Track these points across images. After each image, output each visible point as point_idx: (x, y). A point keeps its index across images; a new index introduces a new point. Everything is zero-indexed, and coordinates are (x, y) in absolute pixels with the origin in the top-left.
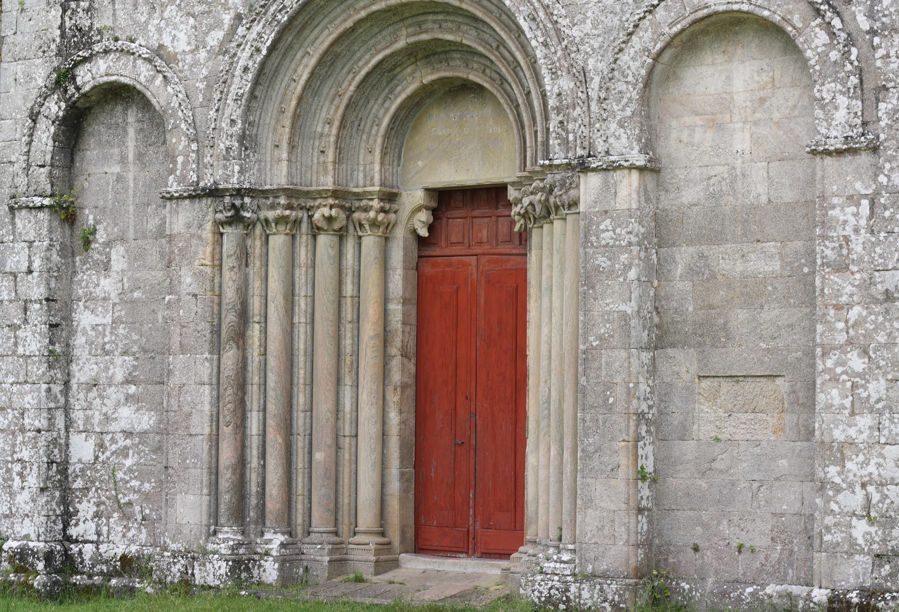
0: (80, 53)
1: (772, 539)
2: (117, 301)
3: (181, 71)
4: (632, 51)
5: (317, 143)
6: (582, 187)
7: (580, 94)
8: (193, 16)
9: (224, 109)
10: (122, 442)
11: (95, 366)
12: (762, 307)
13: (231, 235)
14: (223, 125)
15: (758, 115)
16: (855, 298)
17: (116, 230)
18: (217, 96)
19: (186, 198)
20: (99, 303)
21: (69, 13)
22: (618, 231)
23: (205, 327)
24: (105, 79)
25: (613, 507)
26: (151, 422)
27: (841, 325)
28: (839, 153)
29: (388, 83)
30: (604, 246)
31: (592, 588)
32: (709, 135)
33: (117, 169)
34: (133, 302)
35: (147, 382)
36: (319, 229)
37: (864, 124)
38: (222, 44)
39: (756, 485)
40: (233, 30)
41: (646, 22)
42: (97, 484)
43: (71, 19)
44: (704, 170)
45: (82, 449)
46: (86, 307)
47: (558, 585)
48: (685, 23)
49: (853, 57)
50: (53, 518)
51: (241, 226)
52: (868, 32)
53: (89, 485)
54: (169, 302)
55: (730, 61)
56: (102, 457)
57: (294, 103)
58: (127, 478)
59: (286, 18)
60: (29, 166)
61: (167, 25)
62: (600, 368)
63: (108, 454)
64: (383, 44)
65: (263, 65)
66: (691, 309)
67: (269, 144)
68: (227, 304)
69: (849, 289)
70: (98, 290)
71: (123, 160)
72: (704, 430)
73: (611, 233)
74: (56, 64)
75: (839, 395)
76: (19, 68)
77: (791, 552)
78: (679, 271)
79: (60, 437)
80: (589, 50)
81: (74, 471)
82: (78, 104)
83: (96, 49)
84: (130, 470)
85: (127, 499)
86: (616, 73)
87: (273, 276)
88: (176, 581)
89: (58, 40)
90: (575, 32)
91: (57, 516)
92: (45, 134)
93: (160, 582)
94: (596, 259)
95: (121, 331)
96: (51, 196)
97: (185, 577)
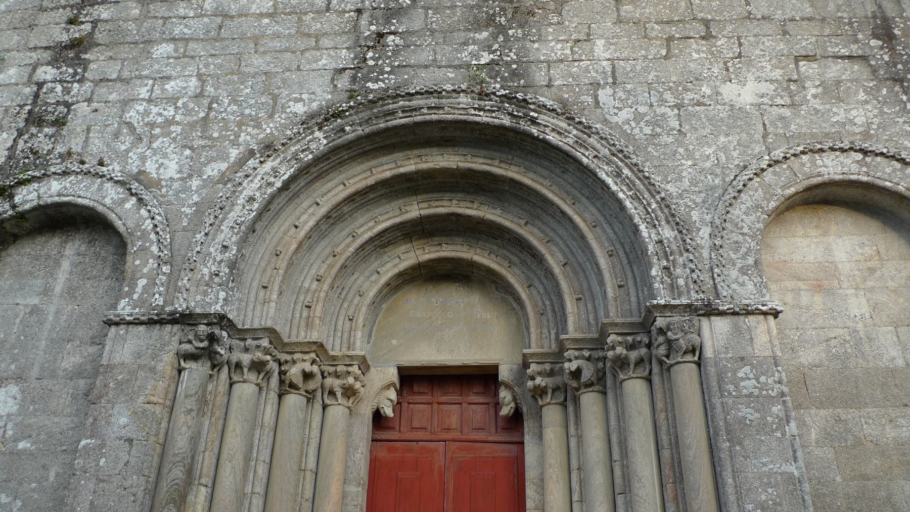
0: (30, 173)
3: (162, 196)
4: (743, 207)
5: (302, 298)
6: (706, 332)
9: (215, 234)
13: (196, 371)
14: (212, 250)
15: (870, 284)
17: (13, 367)
19: (142, 323)
21: (26, 137)
22: (763, 379)
24: (56, 199)
32: (818, 299)
33: (35, 301)
36: (292, 386)
40: (241, 162)
43: (26, 142)
44: (821, 332)
48: (800, 187)
51: (209, 364)
55: (825, 234)
57: (294, 246)
59: (310, 157)
61: (154, 154)
64: (391, 214)
65: (273, 197)
67: (255, 284)
68: (174, 455)
71: (46, 292)
73: (754, 381)
78: (813, 436)
80: (690, 204)
83: (53, 169)
86: (728, 225)
87: (234, 430)
90: (671, 188)
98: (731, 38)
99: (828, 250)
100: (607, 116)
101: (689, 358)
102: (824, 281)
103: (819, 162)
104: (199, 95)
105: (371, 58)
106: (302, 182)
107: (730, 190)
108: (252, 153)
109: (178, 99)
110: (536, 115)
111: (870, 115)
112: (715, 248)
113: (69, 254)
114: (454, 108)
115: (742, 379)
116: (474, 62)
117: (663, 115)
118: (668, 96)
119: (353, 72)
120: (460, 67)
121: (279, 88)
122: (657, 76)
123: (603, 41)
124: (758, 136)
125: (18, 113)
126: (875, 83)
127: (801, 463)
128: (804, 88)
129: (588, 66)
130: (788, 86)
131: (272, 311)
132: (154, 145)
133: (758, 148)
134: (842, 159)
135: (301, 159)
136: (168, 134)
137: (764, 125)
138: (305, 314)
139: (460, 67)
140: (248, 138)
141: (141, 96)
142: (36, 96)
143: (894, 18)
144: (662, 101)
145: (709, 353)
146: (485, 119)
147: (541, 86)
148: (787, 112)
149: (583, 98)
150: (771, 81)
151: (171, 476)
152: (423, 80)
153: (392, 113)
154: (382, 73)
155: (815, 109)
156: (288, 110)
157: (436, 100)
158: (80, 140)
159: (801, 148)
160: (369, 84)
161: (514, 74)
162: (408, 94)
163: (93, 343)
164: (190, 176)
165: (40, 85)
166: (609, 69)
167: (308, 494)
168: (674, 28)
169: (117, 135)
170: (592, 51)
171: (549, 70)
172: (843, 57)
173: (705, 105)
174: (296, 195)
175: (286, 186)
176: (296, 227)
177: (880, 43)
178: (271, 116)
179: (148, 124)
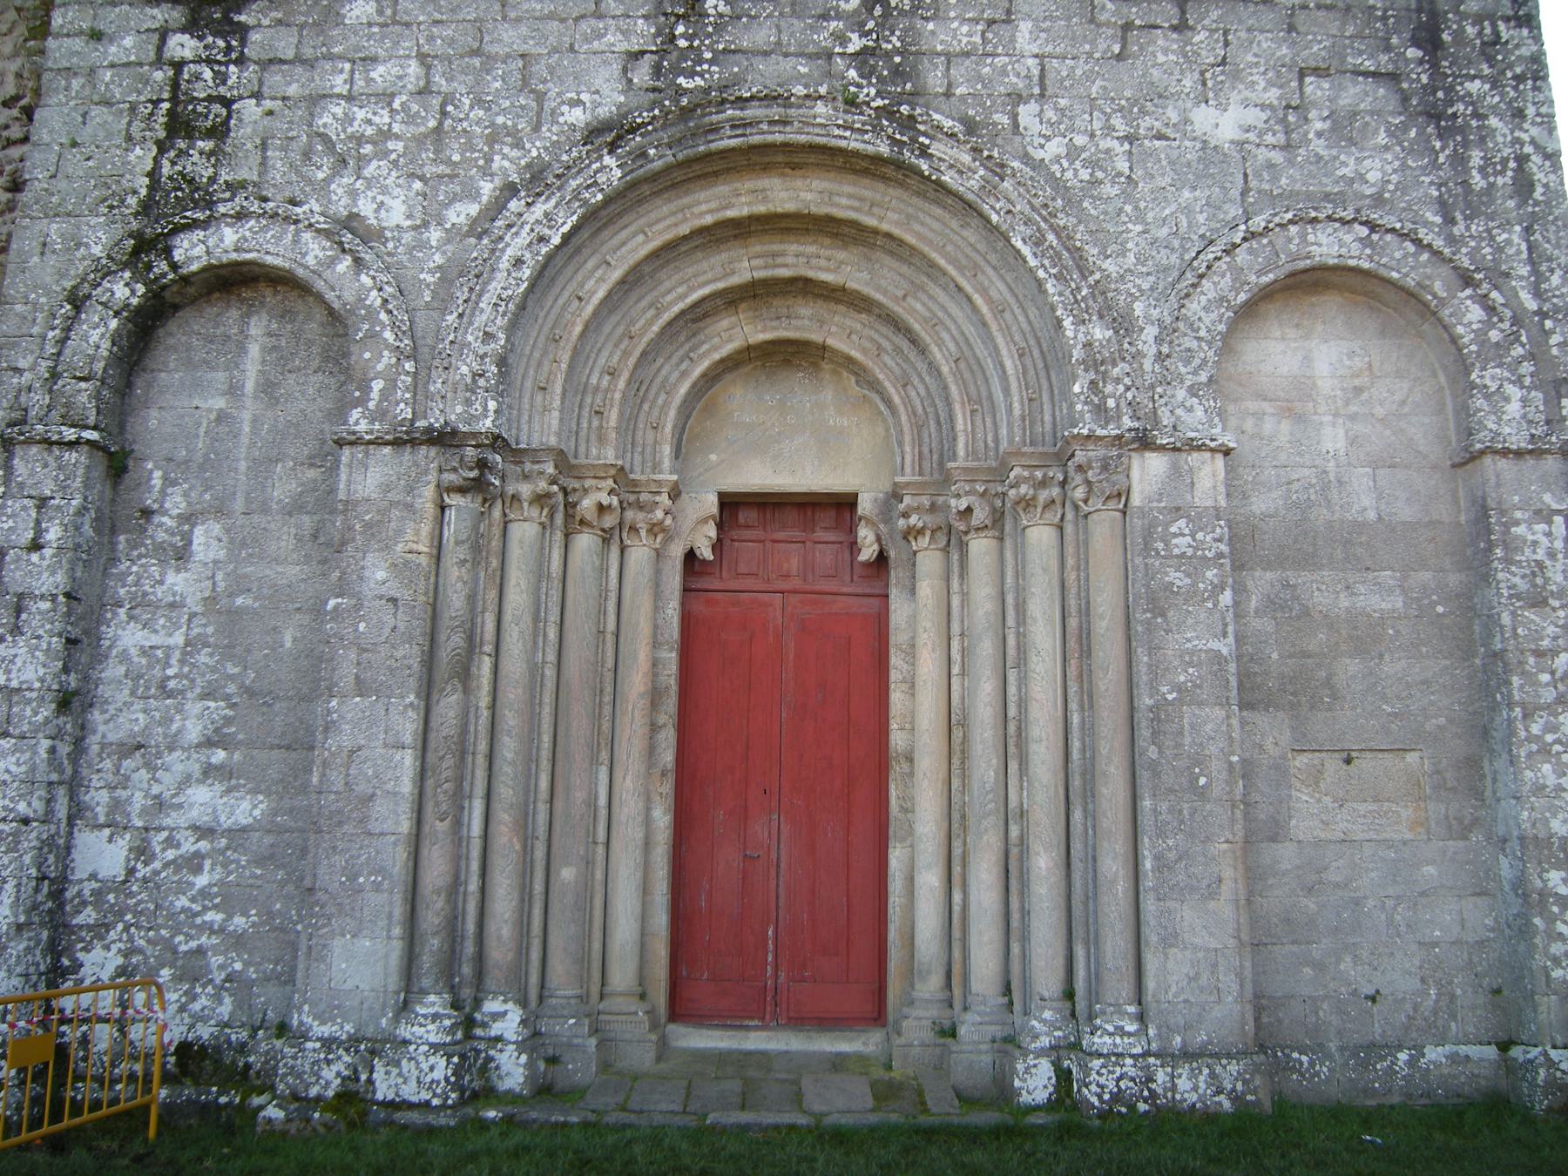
0: (188, 214)
1: (1423, 980)
2: (199, 609)
3: (389, 254)
4: (1203, 299)
5: (589, 400)
6: (1135, 474)
7: (1126, 346)
8: (422, 178)
9: (473, 314)
10: (189, 846)
11: (141, 716)
12: (1381, 656)
14: (470, 338)
15: (1353, 408)
16: (1561, 641)
17: (207, 497)
18: (462, 295)
19: (387, 443)
20: (160, 612)
21: (172, 154)
22: (1200, 536)
23: (410, 654)
24: (234, 256)
25: (1213, 944)
26: (257, 812)
27: (1545, 678)
28: (1519, 454)
29: (688, 339)
30: (1177, 556)
31: (1193, 1075)
32: (1285, 426)
33: (220, 403)
34: (235, 614)
35: (250, 744)
37: (1548, 422)
38: (474, 222)
39: (1390, 903)
40: (496, 207)
41: (1222, 265)
42: (128, 917)
43: (173, 163)
44: (1282, 472)
45: (101, 855)
46: (131, 618)
47: (1132, 1072)
48: (1281, 273)
49: (1524, 339)
50: (35, 978)
51: (480, 499)
52: (1535, 313)
53: (110, 918)
54: (336, 608)
55: (1307, 337)
56: (143, 870)
57: (578, 329)
58: (197, 907)
59: (600, 197)
60: (54, 375)
61: (369, 188)
62: (1181, 733)
63: (157, 865)
64: (710, 276)
65: (550, 257)
66: (1275, 656)
68: (452, 618)
69: (1551, 630)
70: (159, 590)
71: (234, 391)
72: (1303, 826)
73: (1189, 539)
74: (135, 225)
75: (1554, 771)
76: (55, 230)
77: (1453, 997)
78: (1253, 604)
79: (58, 833)
81: (79, 894)
82: (167, 294)
84: (204, 893)
85: (193, 944)
86: (1181, 325)
88: (330, 1093)
89: (144, 192)
90: (1110, 266)
91: (41, 974)
92: (97, 335)
93: (295, 1097)
94: (1167, 574)
95: (203, 658)
96: (95, 428)
97: (352, 1086)
98: (1217, 30)
99: (1307, 360)
100: (1030, 149)
101: (1112, 504)
102: (1295, 403)
103: (1311, 238)
104: (424, 91)
105: (683, 36)
106: (585, 233)
107: (1188, 274)
108: (511, 190)
109: (393, 95)
110: (927, 142)
111: (1389, 169)
112: (1160, 357)
113: (256, 331)
114: (808, 124)
115: (1175, 535)
116: (837, 50)
117: (1108, 151)
118: (1117, 121)
119: (655, 57)
120: (817, 56)
121: (545, 82)
122: (1104, 88)
123: (1030, 24)
124: (1235, 193)
125: (152, 114)
126: (1402, 118)
127: (1231, 639)
128: (1306, 119)
129: (1005, 65)
130: (1286, 116)
131: (555, 423)
132: (366, 173)
133: (1234, 211)
134: (1340, 234)
135: (585, 202)
136: (385, 154)
137: (1246, 175)
138: (596, 423)
139: (817, 56)
140: (506, 164)
141: (337, 90)
142: (175, 85)
143: (1446, 13)
144: (1109, 129)
145: (1136, 500)
146: (854, 145)
147: (936, 95)
148: (1277, 157)
149: (997, 117)
150: (1263, 107)
151: (451, 644)
152: (763, 75)
153: (714, 129)
154: (700, 61)
155: (1317, 155)
156: (561, 120)
157: (781, 110)
158: (256, 158)
159: (1289, 216)
160: (681, 80)
161: (898, 73)
162: (739, 99)
163: (312, 465)
164: (426, 224)
165: (179, 66)
166: (1036, 72)
167: (610, 663)
168: (1134, 10)
169: (307, 155)
170: (1013, 40)
171: (948, 69)
172: (1366, 74)
173: (1167, 139)
174: (578, 251)
175: (567, 238)
176: (580, 299)
177: (1420, 54)
178: (537, 128)
179: (351, 137)
